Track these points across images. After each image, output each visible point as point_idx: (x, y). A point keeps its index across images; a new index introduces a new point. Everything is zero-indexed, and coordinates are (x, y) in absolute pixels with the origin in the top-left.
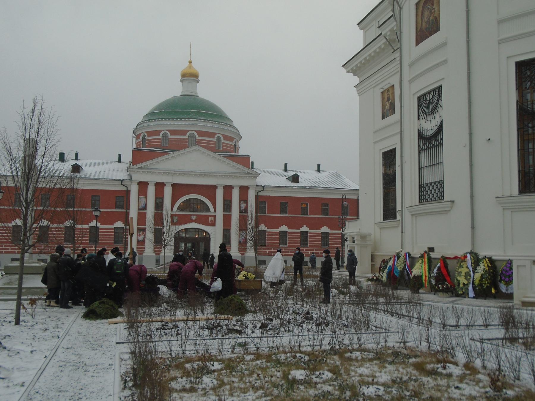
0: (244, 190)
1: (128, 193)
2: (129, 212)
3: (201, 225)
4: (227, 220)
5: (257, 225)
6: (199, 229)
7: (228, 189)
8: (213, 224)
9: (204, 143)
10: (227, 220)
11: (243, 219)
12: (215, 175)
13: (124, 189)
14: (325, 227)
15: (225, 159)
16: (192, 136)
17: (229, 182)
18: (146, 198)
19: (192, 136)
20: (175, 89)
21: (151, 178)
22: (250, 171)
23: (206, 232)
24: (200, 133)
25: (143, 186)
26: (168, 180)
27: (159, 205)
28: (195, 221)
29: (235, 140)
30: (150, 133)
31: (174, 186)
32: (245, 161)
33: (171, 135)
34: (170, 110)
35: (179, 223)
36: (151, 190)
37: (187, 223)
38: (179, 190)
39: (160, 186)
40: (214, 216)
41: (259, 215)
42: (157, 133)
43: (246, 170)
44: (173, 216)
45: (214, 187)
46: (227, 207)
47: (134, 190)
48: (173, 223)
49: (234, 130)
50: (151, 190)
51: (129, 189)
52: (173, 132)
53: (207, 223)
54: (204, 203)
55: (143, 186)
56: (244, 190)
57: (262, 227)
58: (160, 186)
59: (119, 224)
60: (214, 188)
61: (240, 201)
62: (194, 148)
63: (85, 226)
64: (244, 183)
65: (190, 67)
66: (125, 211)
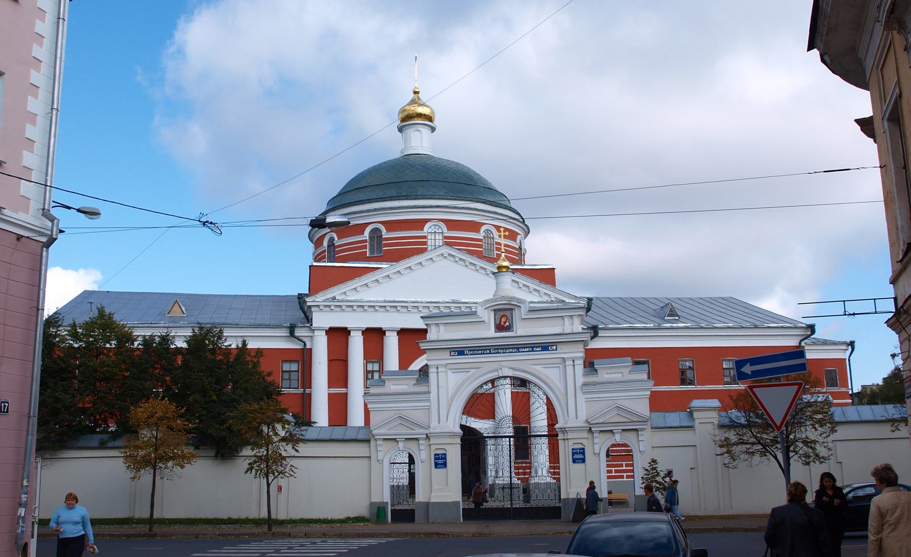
2: (310, 394)
13: (298, 346)
21: (356, 321)
25: (339, 335)
31: (402, 333)
33: (388, 230)
51: (308, 347)
52: (391, 225)
55: (339, 335)
58: (374, 336)
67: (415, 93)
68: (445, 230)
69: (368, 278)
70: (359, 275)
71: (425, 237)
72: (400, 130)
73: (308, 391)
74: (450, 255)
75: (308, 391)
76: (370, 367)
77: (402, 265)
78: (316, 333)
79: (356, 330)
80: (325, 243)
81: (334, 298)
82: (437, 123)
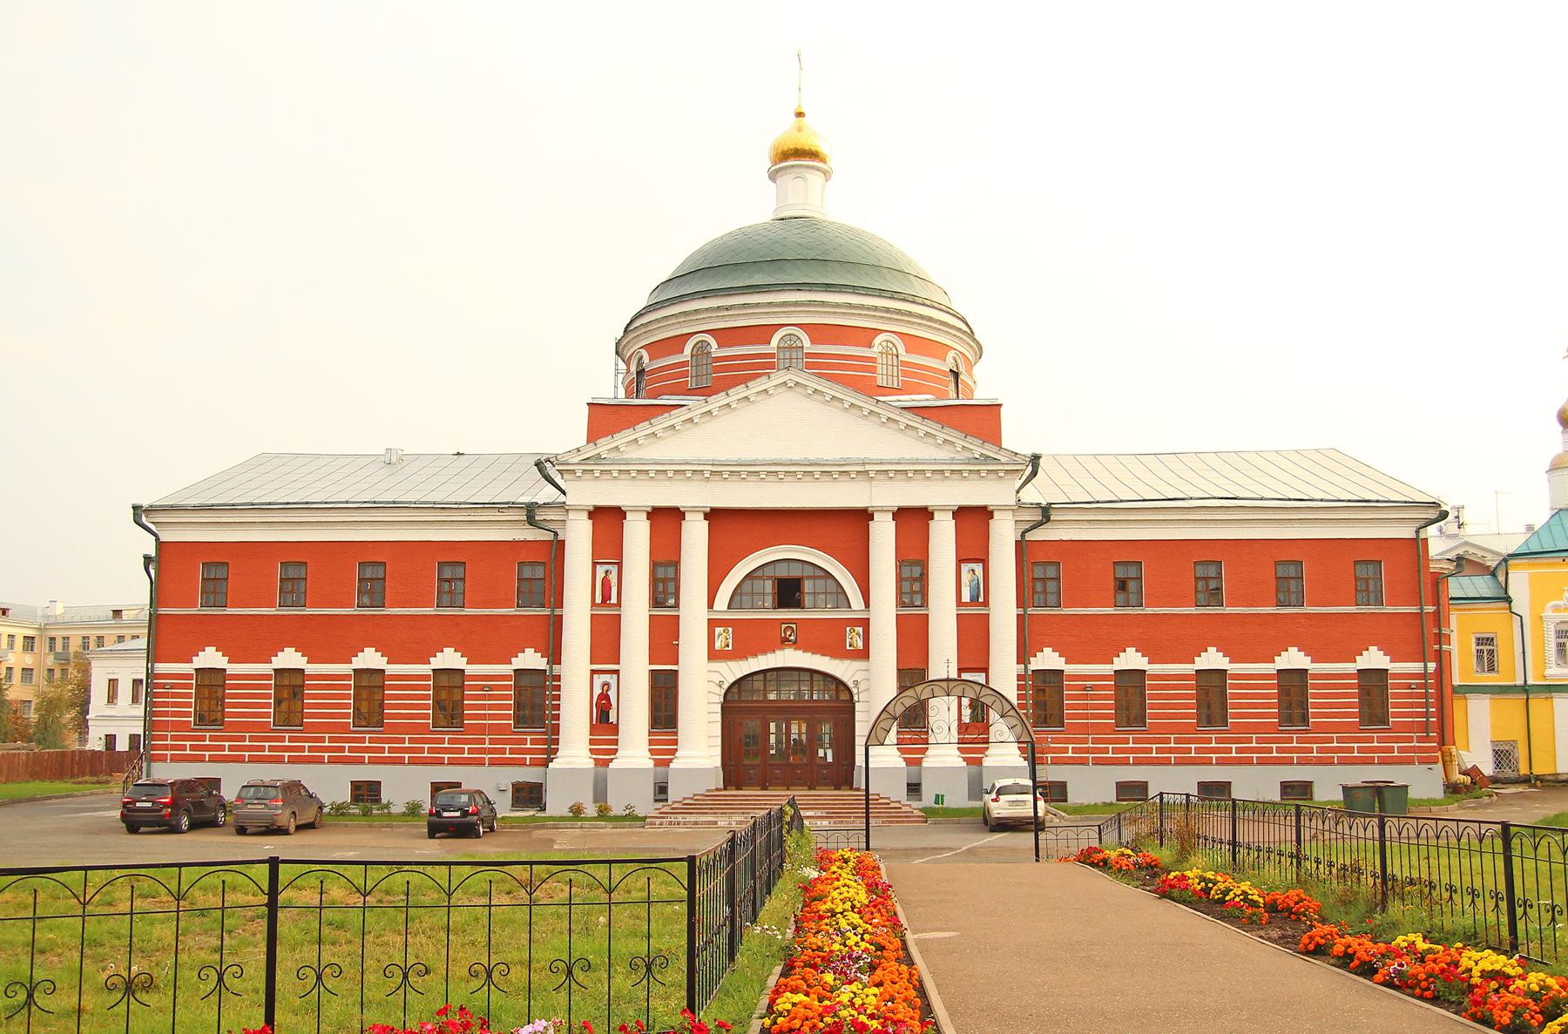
0: (974, 520)
1: (557, 548)
3: (818, 657)
4: (913, 633)
5: (1024, 652)
6: (812, 672)
8: (864, 654)
9: (829, 366)
10: (913, 633)
11: (974, 634)
12: (864, 472)
14: (1293, 650)
15: (916, 421)
16: (791, 347)
18: (620, 565)
19: (791, 347)
20: (746, 205)
21: (636, 496)
22: (990, 451)
23: (839, 683)
24: (818, 332)
25: (608, 519)
26: (695, 497)
27: (664, 588)
29: (951, 354)
30: (656, 349)
31: (715, 516)
32: (982, 421)
33: (720, 345)
34: (724, 270)
35: (739, 652)
36: (637, 535)
37: (764, 652)
38: (731, 527)
40: (865, 624)
41: (1030, 611)
42: (677, 343)
43: (978, 448)
44: (712, 624)
47: (579, 537)
48: (714, 655)
49: (965, 328)
50: (637, 535)
53: (839, 651)
54: (829, 575)
55: (608, 519)
56: (974, 520)
57: (1048, 659)
58: (666, 519)
59: (531, 659)
60: (863, 516)
61: (960, 561)
62: (779, 377)
63: (424, 669)
64: (972, 494)
65: (799, 130)
66: (547, 612)
67: (800, 115)
68: (807, 343)
69: (660, 423)
70: (631, 424)
71: (873, 360)
72: (773, 176)
73: (558, 612)
75: (558, 612)
76: (661, 573)
77: (718, 400)
78: (572, 515)
79: (636, 510)
80: (633, 369)
82: (832, 163)
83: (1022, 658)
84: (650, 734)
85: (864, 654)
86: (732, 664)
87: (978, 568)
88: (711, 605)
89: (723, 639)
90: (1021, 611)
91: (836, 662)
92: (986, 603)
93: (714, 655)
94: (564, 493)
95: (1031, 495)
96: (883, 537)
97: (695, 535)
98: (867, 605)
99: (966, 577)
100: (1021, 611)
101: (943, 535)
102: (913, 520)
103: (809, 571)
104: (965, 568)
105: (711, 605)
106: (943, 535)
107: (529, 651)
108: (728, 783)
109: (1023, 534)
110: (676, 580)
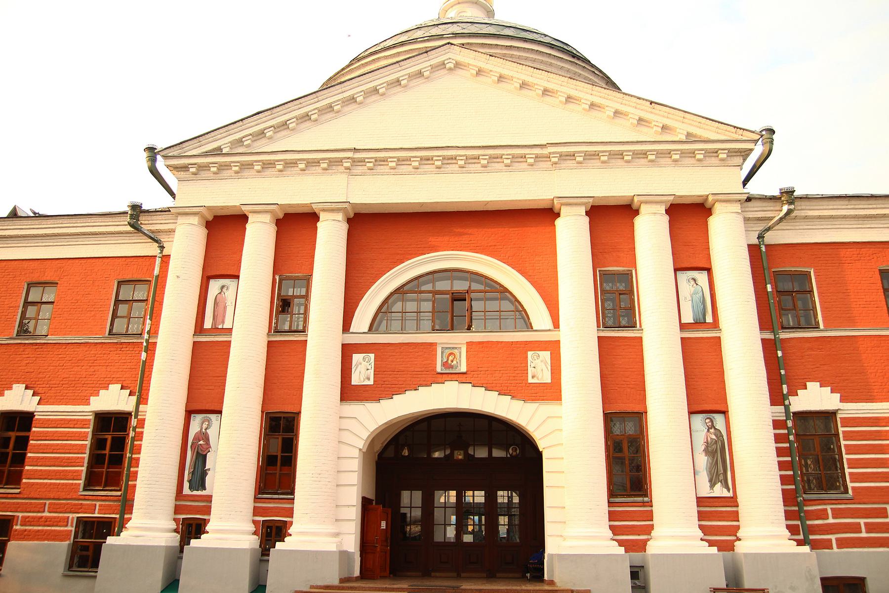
4: (620, 366)
7: (611, 219)
8: (551, 392)
10: (620, 366)
13: (151, 249)
17: (612, 185)
25: (224, 228)
28: (461, 377)
36: (258, 243)
38: (375, 231)
39: (296, 224)
44: (348, 351)
45: (548, 214)
46: (616, 299)
47: (186, 246)
48: (349, 392)
50: (258, 243)
54: (503, 292)
58: (296, 224)
59: (113, 399)
64: (689, 184)
74: (458, 65)
81: (219, 149)
83: (777, 398)
84: (256, 499)
85: (551, 392)
86: (371, 406)
87: (702, 277)
88: (346, 328)
89: (363, 370)
90: (769, 336)
91: (518, 404)
92: (715, 325)
93: (349, 392)
94: (172, 194)
95: (766, 183)
96: (572, 235)
97: (330, 237)
98: (556, 325)
99: (686, 289)
100: (769, 336)
101: (651, 235)
102: (611, 219)
103: (475, 286)
104: (683, 276)
105: (346, 328)
106: (651, 235)
107: (115, 388)
108: (366, 573)
109: (761, 237)
110: (307, 297)
